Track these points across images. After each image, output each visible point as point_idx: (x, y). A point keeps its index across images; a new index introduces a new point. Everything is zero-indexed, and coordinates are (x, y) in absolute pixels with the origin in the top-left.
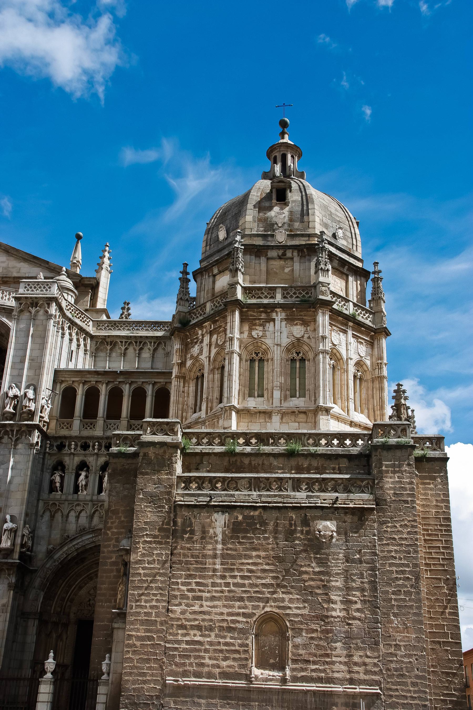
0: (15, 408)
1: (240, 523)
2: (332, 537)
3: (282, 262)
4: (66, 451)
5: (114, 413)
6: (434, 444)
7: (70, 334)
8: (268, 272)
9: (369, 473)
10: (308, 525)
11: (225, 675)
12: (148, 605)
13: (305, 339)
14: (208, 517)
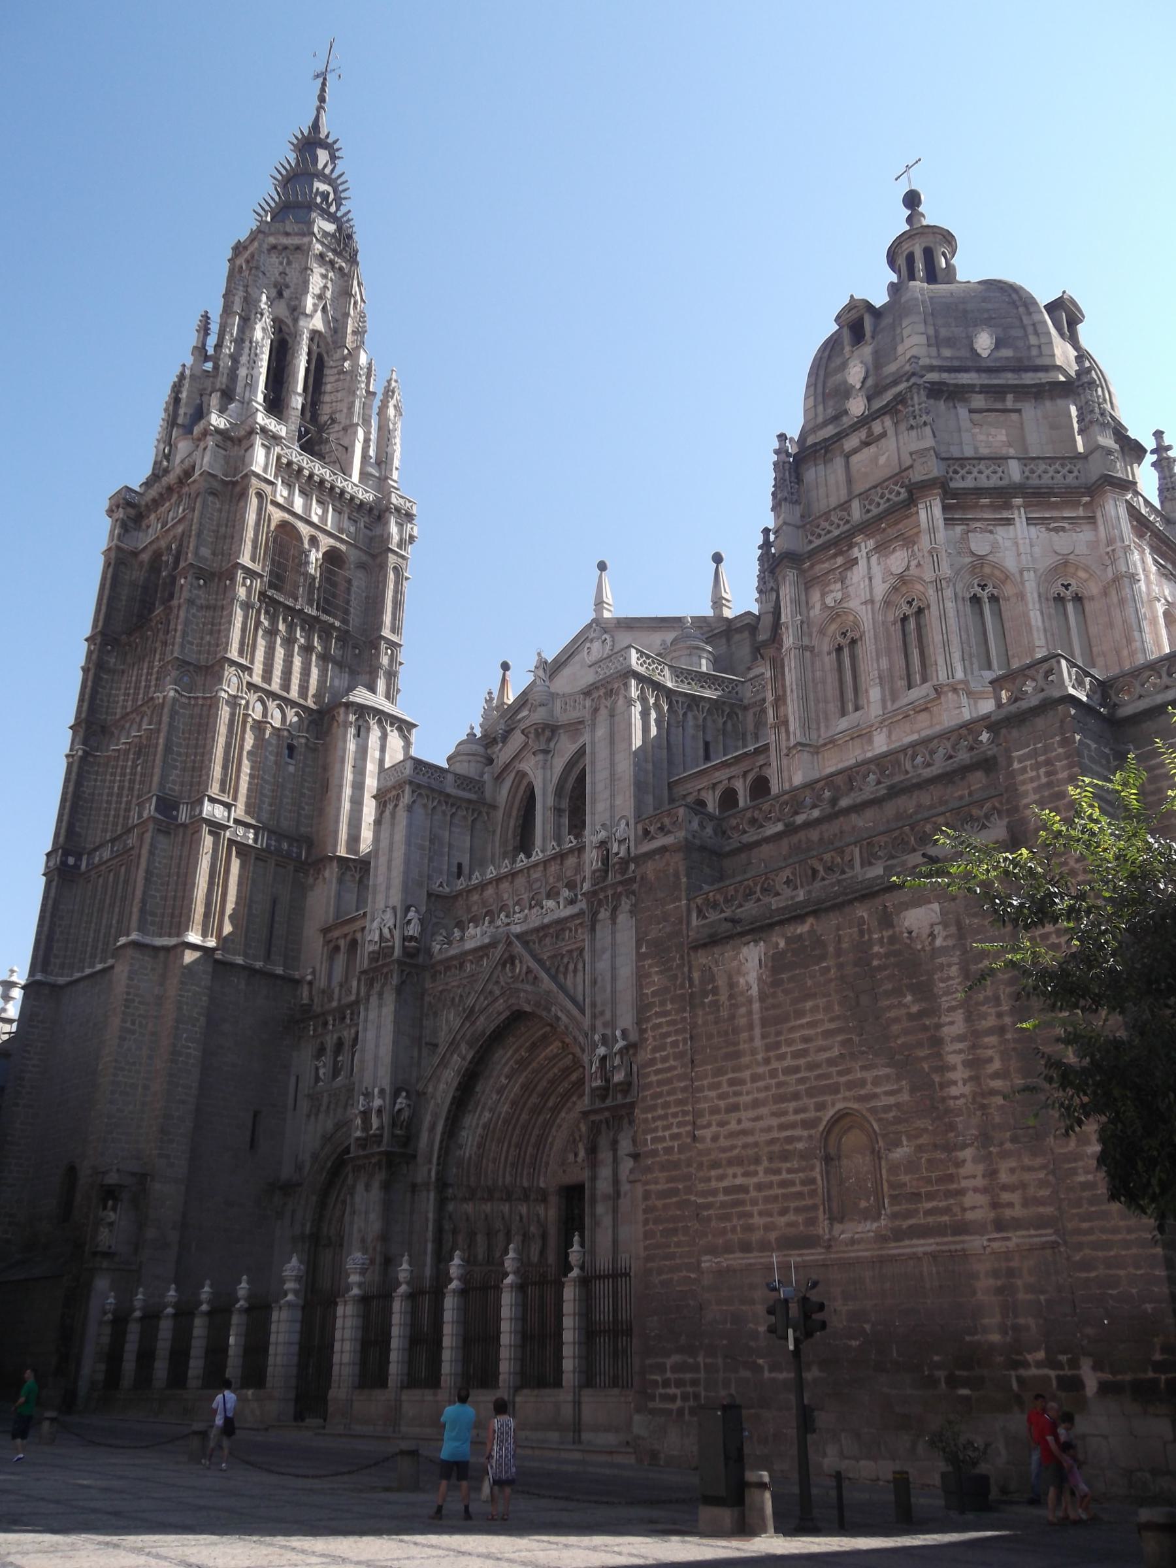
0: (605, 860)
1: (782, 954)
2: (932, 935)
3: (873, 449)
6: (1164, 675)
7: (695, 718)
11: (788, 1243)
12: (667, 1134)
13: (913, 571)
14: (734, 958)
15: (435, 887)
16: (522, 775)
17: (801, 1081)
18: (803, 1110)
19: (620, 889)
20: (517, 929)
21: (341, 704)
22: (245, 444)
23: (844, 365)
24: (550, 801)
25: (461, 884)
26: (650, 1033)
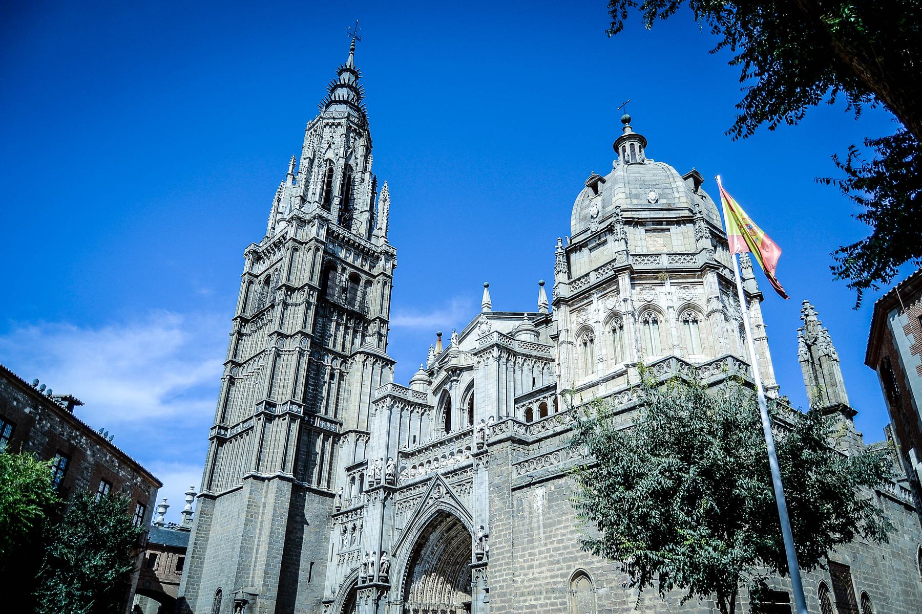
3: (602, 248)
15: (402, 449)
16: (446, 391)
17: (561, 554)
18: (561, 569)
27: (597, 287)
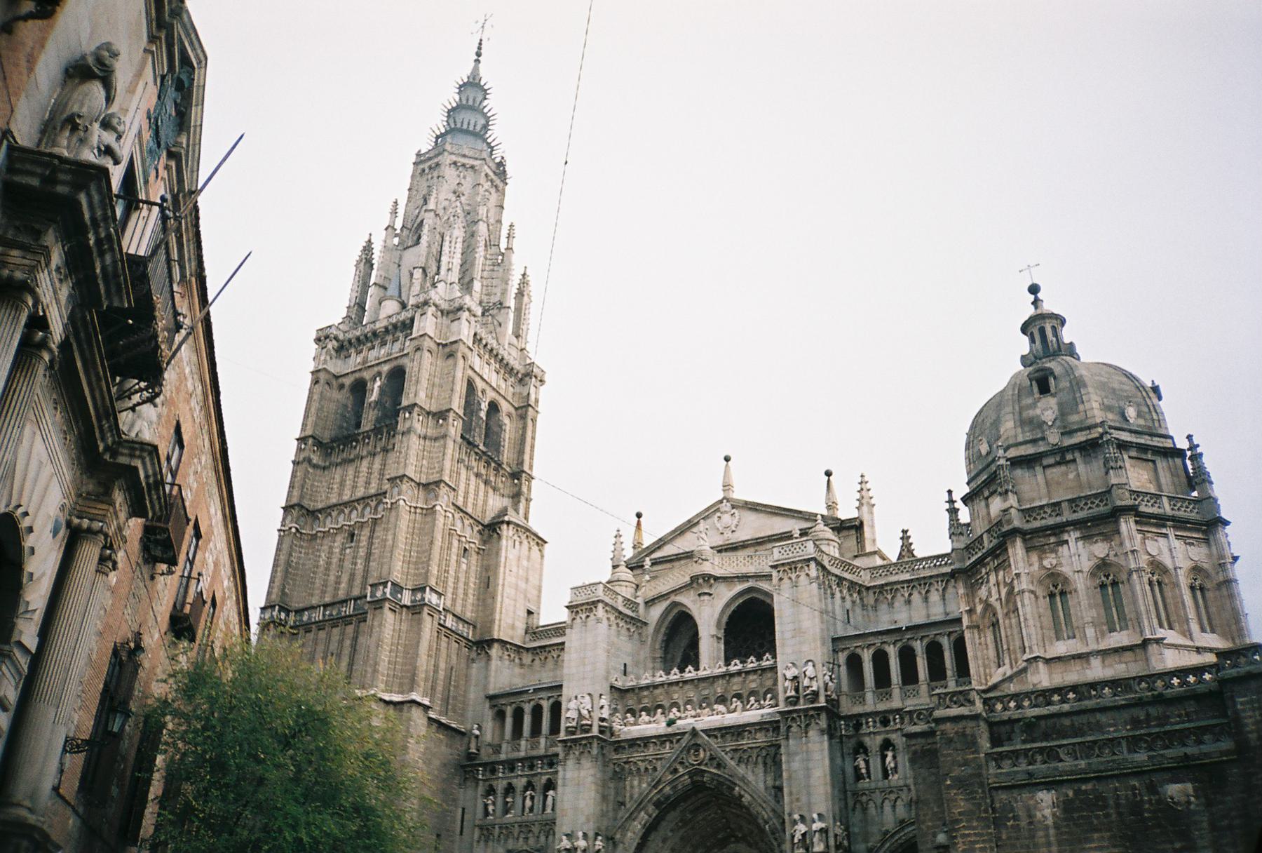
0: (797, 690)
3: (1063, 468)
4: (864, 730)
5: (910, 676)
7: (841, 591)
8: (1047, 483)
9: (1226, 716)
10: (1157, 793)
14: (1032, 798)
19: (812, 713)
20: (700, 726)
21: (503, 522)
22: (451, 316)
23: (1034, 406)
24: (713, 631)
25: (630, 684)
26: (960, 840)
27: (1076, 524)
